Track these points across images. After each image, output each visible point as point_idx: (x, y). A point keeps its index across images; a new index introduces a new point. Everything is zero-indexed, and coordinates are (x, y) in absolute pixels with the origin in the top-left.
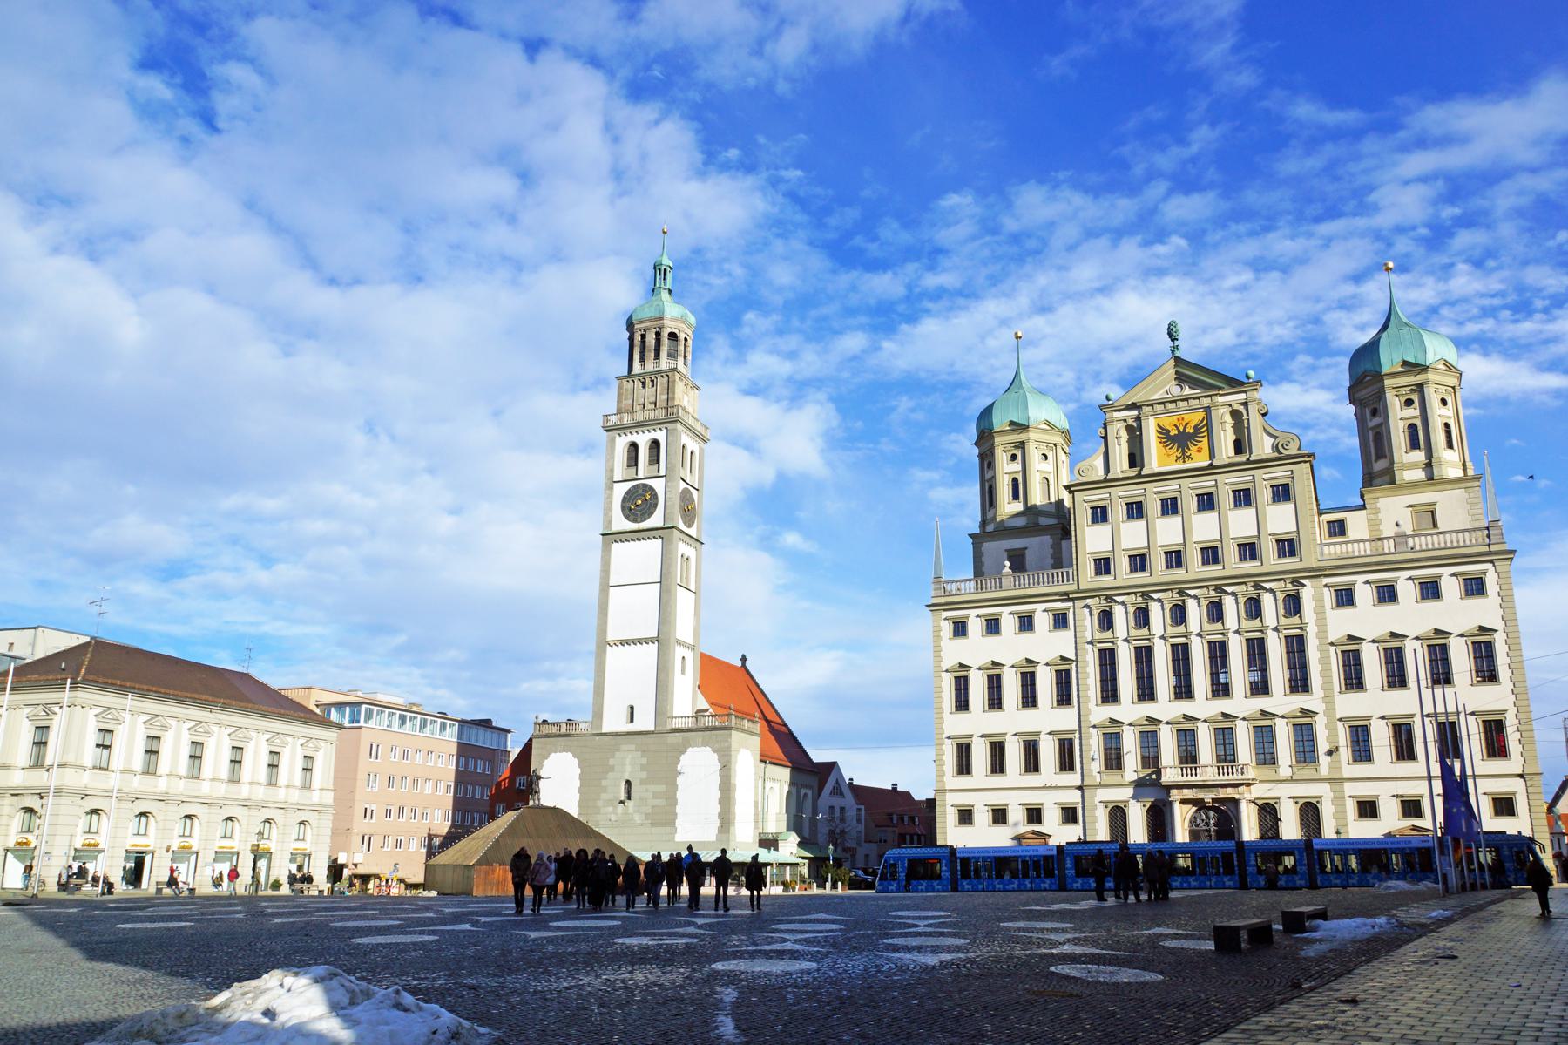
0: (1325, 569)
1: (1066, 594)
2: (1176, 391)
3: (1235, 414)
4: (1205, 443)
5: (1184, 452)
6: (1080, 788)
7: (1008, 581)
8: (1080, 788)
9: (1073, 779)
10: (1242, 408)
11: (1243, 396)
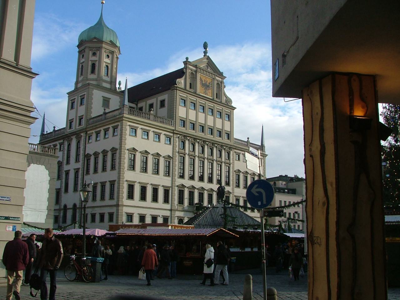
0: (236, 147)
1: (173, 130)
2: (206, 68)
3: (218, 84)
4: (210, 91)
5: (206, 91)
6: (171, 210)
7: (152, 117)
8: (171, 210)
9: (168, 206)
10: (220, 83)
11: (220, 79)
